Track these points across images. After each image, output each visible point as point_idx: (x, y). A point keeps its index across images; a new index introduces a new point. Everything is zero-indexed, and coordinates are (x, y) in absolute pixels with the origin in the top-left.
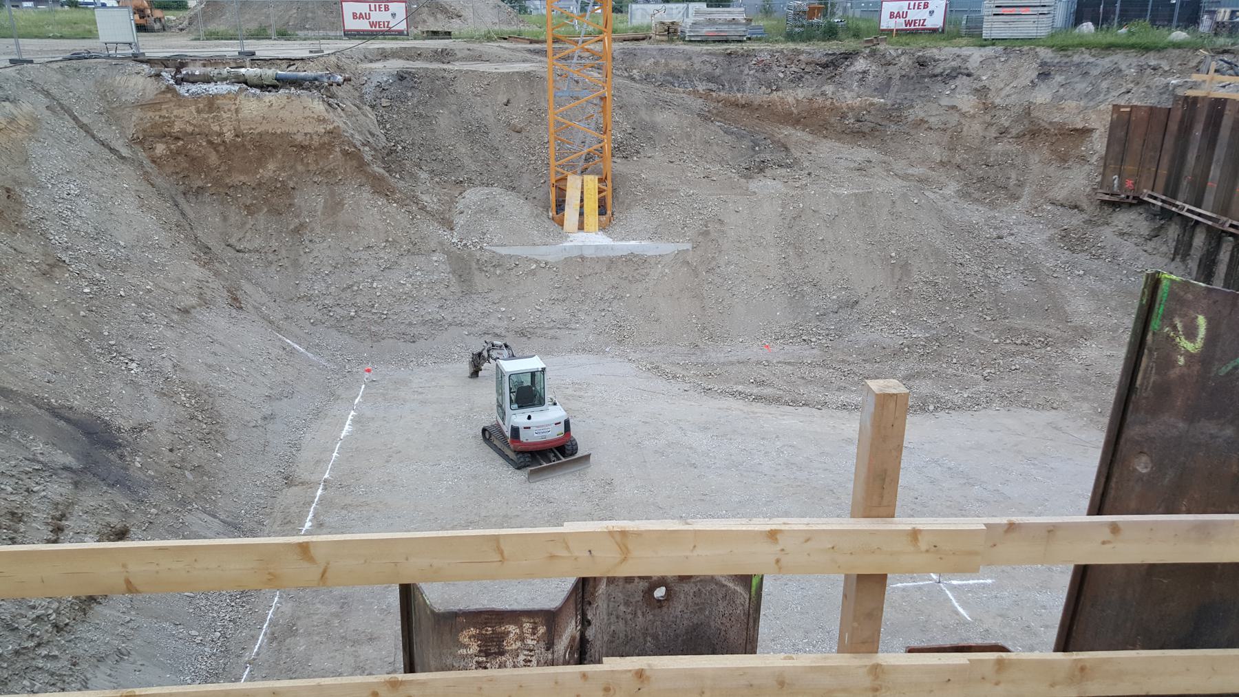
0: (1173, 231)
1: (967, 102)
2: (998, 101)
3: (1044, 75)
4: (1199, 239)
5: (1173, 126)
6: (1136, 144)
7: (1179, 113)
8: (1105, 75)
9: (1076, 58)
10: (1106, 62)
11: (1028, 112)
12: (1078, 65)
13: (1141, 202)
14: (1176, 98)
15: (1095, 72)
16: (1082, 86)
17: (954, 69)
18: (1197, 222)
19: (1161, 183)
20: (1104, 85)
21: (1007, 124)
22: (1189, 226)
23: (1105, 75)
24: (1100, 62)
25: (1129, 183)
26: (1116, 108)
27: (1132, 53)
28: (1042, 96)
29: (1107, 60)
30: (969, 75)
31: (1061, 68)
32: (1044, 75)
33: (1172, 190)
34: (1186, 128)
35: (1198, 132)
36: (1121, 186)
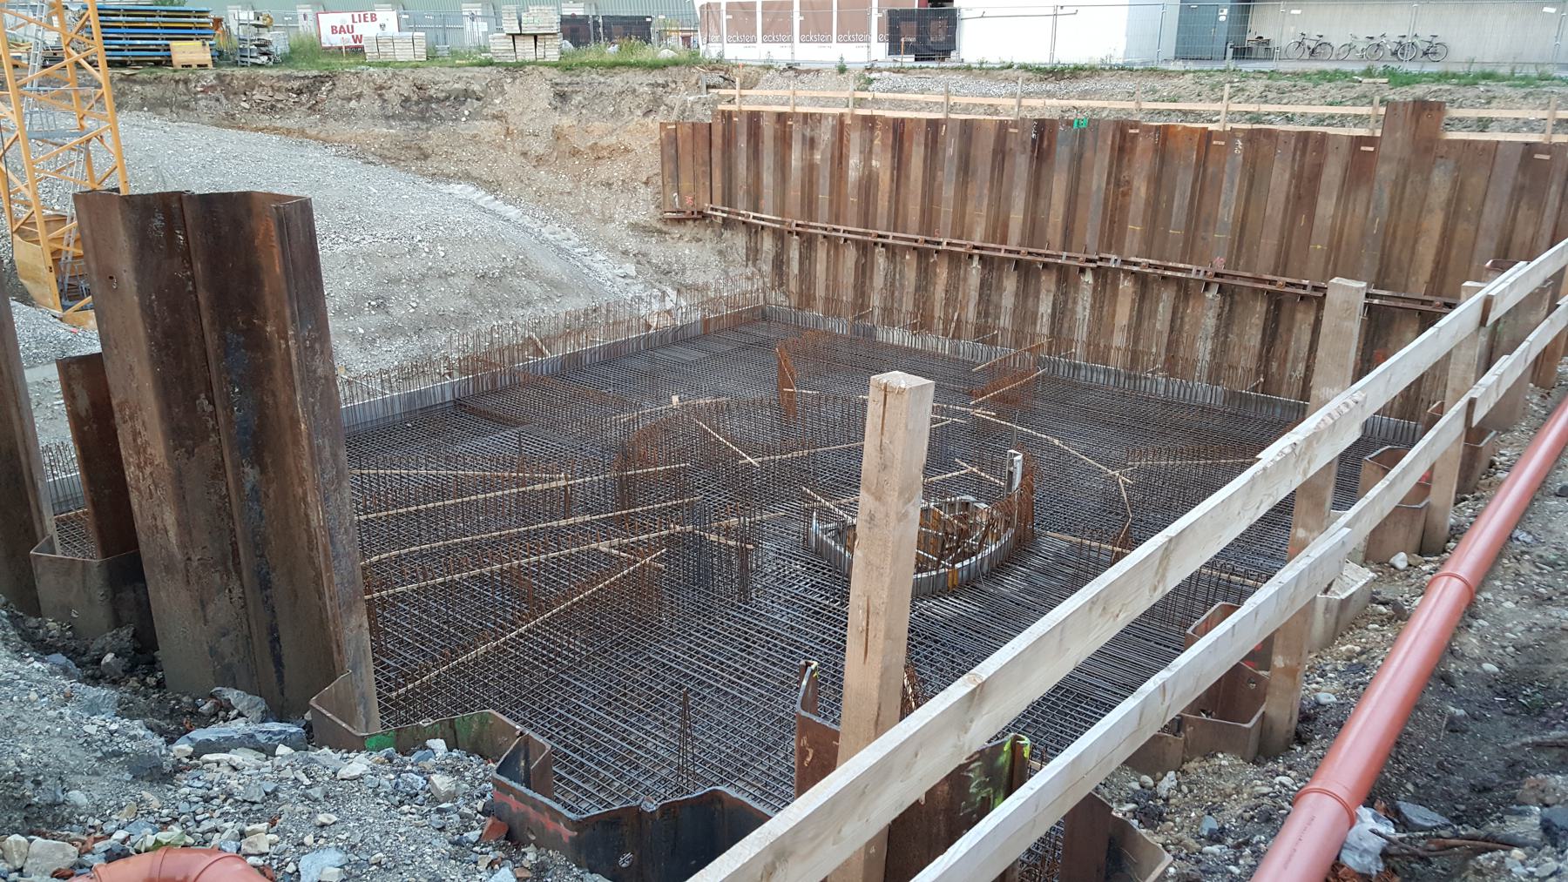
0: (740, 240)
3: (562, 97)
4: (768, 244)
5: (717, 140)
6: (686, 161)
7: (720, 127)
10: (618, 81)
13: (705, 217)
22: (753, 230)
25: (689, 199)
27: (639, 72)
29: (617, 79)
33: (728, 199)
35: (742, 143)
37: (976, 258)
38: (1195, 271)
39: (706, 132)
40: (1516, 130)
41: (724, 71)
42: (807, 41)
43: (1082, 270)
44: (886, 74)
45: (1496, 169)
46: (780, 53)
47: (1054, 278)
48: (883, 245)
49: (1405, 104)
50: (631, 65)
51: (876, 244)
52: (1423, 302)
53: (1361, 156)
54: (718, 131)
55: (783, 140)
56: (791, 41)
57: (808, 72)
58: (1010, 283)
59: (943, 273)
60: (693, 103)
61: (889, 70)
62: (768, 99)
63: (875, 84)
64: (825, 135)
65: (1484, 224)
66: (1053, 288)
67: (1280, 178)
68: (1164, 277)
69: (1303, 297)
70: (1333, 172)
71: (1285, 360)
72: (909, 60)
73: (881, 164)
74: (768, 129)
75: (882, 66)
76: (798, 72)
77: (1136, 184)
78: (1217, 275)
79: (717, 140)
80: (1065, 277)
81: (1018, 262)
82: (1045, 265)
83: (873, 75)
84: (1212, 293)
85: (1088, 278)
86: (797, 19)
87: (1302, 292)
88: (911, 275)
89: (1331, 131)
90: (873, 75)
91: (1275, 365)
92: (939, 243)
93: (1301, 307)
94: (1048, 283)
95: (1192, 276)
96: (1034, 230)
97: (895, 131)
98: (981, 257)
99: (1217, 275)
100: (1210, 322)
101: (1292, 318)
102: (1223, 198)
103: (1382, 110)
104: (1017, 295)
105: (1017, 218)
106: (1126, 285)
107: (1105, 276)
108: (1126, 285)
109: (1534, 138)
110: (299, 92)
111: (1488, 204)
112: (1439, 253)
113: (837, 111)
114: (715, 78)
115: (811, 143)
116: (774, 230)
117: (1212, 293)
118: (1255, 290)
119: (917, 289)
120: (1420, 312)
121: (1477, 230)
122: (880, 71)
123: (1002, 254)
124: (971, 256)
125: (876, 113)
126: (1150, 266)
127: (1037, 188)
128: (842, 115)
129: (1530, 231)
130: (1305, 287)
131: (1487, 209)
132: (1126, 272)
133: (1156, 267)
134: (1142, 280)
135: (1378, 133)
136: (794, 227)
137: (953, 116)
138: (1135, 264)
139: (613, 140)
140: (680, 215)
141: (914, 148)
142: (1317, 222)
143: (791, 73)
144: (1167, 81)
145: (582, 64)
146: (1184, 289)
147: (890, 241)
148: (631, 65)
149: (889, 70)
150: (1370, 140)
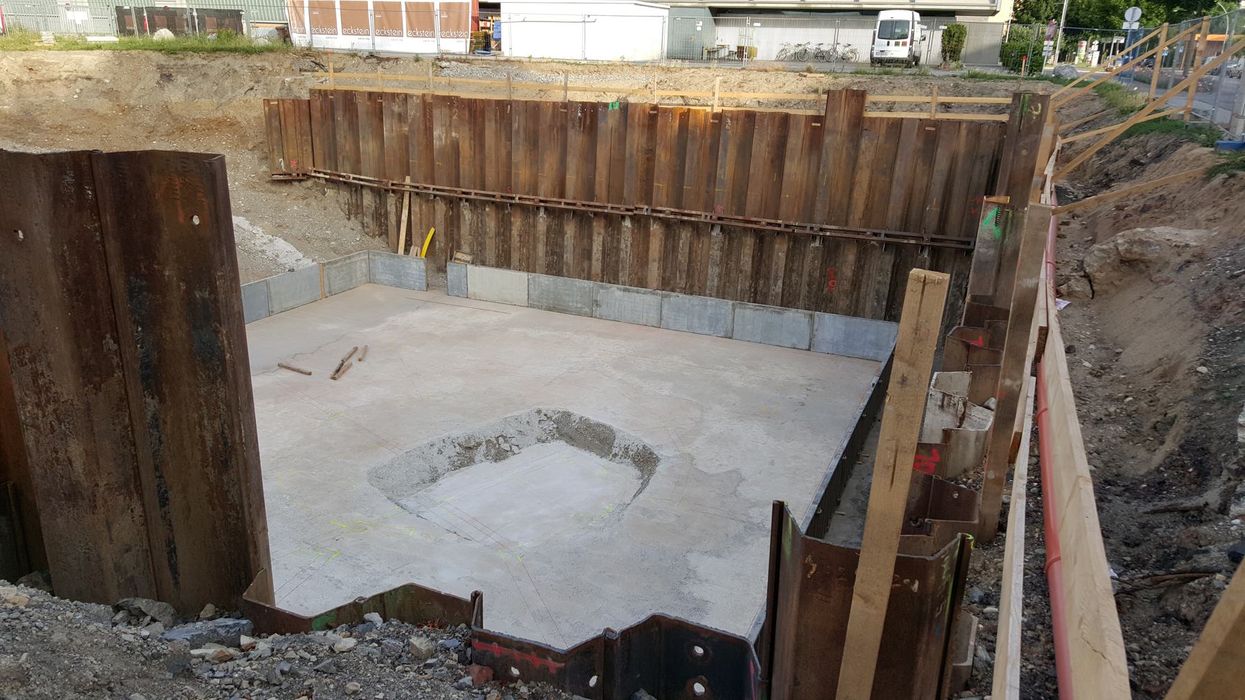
2: (132, 102)
6: (291, 130)
7: (318, 103)
9: (188, 61)
10: (219, 64)
11: (166, 109)
12: (195, 67)
14: (312, 92)
15: (213, 73)
16: (206, 86)
18: (362, 186)
19: (319, 160)
20: (227, 83)
21: (152, 124)
24: (212, 63)
26: (267, 102)
28: (174, 95)
29: (218, 62)
31: (182, 70)
32: (167, 77)
34: (329, 113)
36: (287, 166)
37: (542, 210)
38: (702, 216)
39: (305, 107)
40: (912, 110)
41: (314, 58)
42: (414, 35)
43: (623, 217)
45: (902, 137)
46: (363, 43)
47: (602, 225)
48: (467, 200)
50: (231, 50)
51: (461, 199)
52: (858, 233)
53: (817, 128)
54: (317, 104)
55: (379, 114)
56: (336, 33)
57: (388, 59)
58: (570, 229)
59: (517, 223)
60: (291, 83)
63: (446, 71)
64: (413, 112)
65: (896, 176)
66: (602, 231)
67: (761, 147)
68: (682, 222)
69: (778, 233)
70: (796, 141)
71: (768, 279)
73: (463, 136)
74: (363, 106)
76: (380, 60)
77: (657, 151)
78: (719, 219)
79: (316, 114)
80: (612, 222)
81: (574, 212)
82: (596, 214)
83: (444, 64)
84: (716, 232)
85: (627, 223)
86: (338, 13)
87: (777, 229)
88: (491, 224)
90: (444, 64)
91: (761, 282)
92: (513, 198)
93: (778, 240)
94: (598, 228)
95: (702, 219)
96: (589, 190)
97: (470, 110)
98: (546, 208)
99: (719, 219)
100: (716, 253)
101: (772, 249)
103: (825, 97)
104: (575, 238)
105: (572, 179)
106: (655, 228)
107: (639, 221)
108: (655, 228)
109: (924, 116)
111: (898, 162)
112: (868, 198)
113: (419, 92)
114: (307, 63)
115: (401, 118)
116: (372, 189)
117: (716, 232)
118: (745, 229)
119: (498, 234)
120: (858, 240)
121: (891, 182)
122: (448, 60)
123: (563, 206)
124: (538, 208)
125: (452, 94)
126: (672, 213)
127: (590, 156)
128: (424, 95)
129: (925, 181)
130: (779, 225)
131: (897, 168)
132: (656, 219)
133: (675, 214)
134: (666, 223)
135: (823, 114)
136: (390, 187)
137: (515, 97)
138: (661, 212)
139: (219, 114)
140: (287, 178)
141: (487, 123)
142: (785, 178)
143: (374, 60)
144: (669, 75)
145: (185, 49)
146: (698, 229)
147: (472, 196)
148: (231, 50)
150: (817, 118)
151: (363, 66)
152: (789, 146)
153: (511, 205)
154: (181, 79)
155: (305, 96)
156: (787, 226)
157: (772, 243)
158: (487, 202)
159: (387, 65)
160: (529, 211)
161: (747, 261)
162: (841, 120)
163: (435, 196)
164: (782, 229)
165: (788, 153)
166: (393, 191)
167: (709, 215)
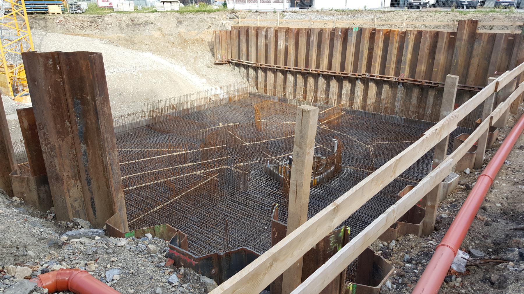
1: (156, 34)
2: (167, 33)
8: (201, 21)
9: (188, 16)
10: (199, 16)
11: (179, 35)
17: (146, 22)
18: (249, 66)
21: (173, 41)
22: (247, 67)
23: (201, 21)
24: (196, 17)
27: (206, 13)
28: (182, 29)
29: (199, 16)
30: (152, 24)
32: (180, 22)
37: (321, 75)
39: (229, 34)
40: (502, 29)
44: (290, 13)
45: (496, 42)
48: (290, 71)
49: (465, 21)
50: (204, 11)
57: (263, 13)
61: (291, 12)
62: (251, 22)
63: (286, 17)
65: (491, 61)
68: (384, 81)
69: (431, 87)
72: (297, 9)
75: (288, 10)
76: (260, 13)
82: (344, 77)
83: (285, 14)
87: (430, 85)
89: (440, 30)
90: (285, 14)
91: (421, 110)
92: (309, 70)
93: (430, 90)
101: (427, 94)
102: (404, 53)
109: (508, 32)
110: (92, 22)
111: (493, 54)
118: (415, 84)
120: (470, 91)
121: (489, 64)
123: (330, 74)
129: (507, 63)
130: (431, 83)
131: (492, 57)
133: (381, 77)
138: (374, 76)
139: (198, 37)
142: (435, 61)
143: (258, 13)
144: (384, 14)
145: (187, 11)
148: (204, 11)
149: (291, 12)
150: (452, 33)
151: (254, 16)
152: (438, 46)
153: (308, 73)
154: (185, 23)
155: (230, 29)
156: (435, 84)
157: (428, 91)
158: (298, 72)
159: (263, 15)
160: (316, 76)
161: (414, 100)
162: (465, 35)
163: (277, 70)
164: (433, 85)
165: (437, 50)
166: (261, 68)
167: (397, 78)
